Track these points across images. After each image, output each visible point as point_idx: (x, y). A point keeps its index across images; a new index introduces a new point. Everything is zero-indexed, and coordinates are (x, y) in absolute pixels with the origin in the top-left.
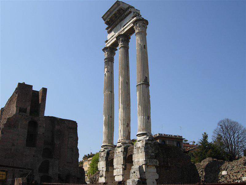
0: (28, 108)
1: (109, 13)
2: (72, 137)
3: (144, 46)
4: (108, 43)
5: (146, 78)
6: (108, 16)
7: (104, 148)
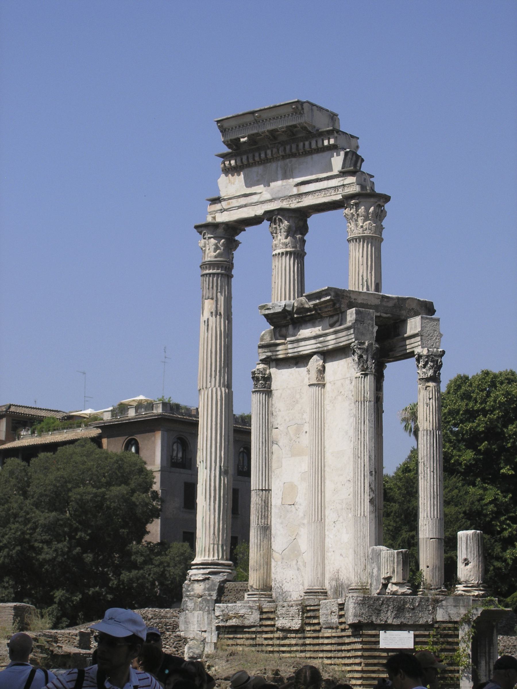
1: (250, 118)
4: (222, 211)
6: (243, 126)
7: (207, 571)
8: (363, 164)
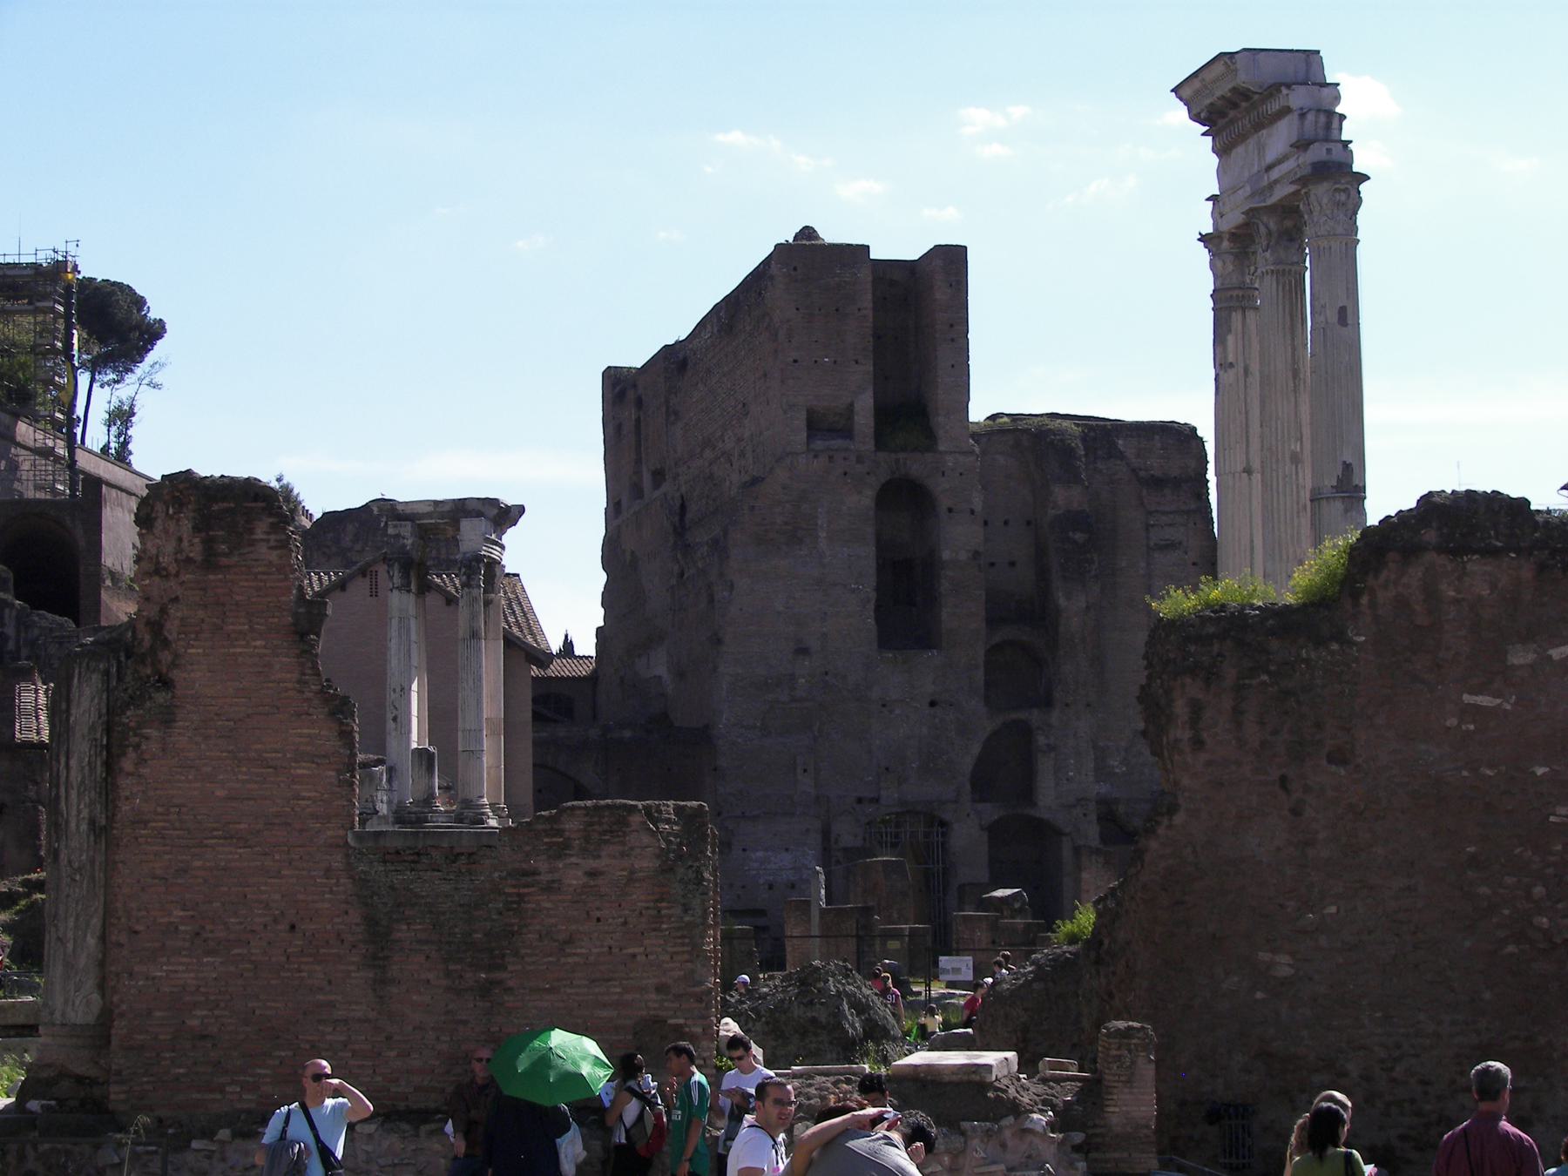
0: (857, 407)
2: (1170, 546)
3: (1342, 311)
5: (1347, 467)
8: (1345, 123)
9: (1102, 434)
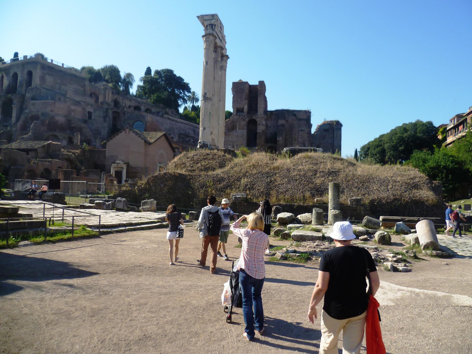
2: (302, 130)
9: (288, 111)
